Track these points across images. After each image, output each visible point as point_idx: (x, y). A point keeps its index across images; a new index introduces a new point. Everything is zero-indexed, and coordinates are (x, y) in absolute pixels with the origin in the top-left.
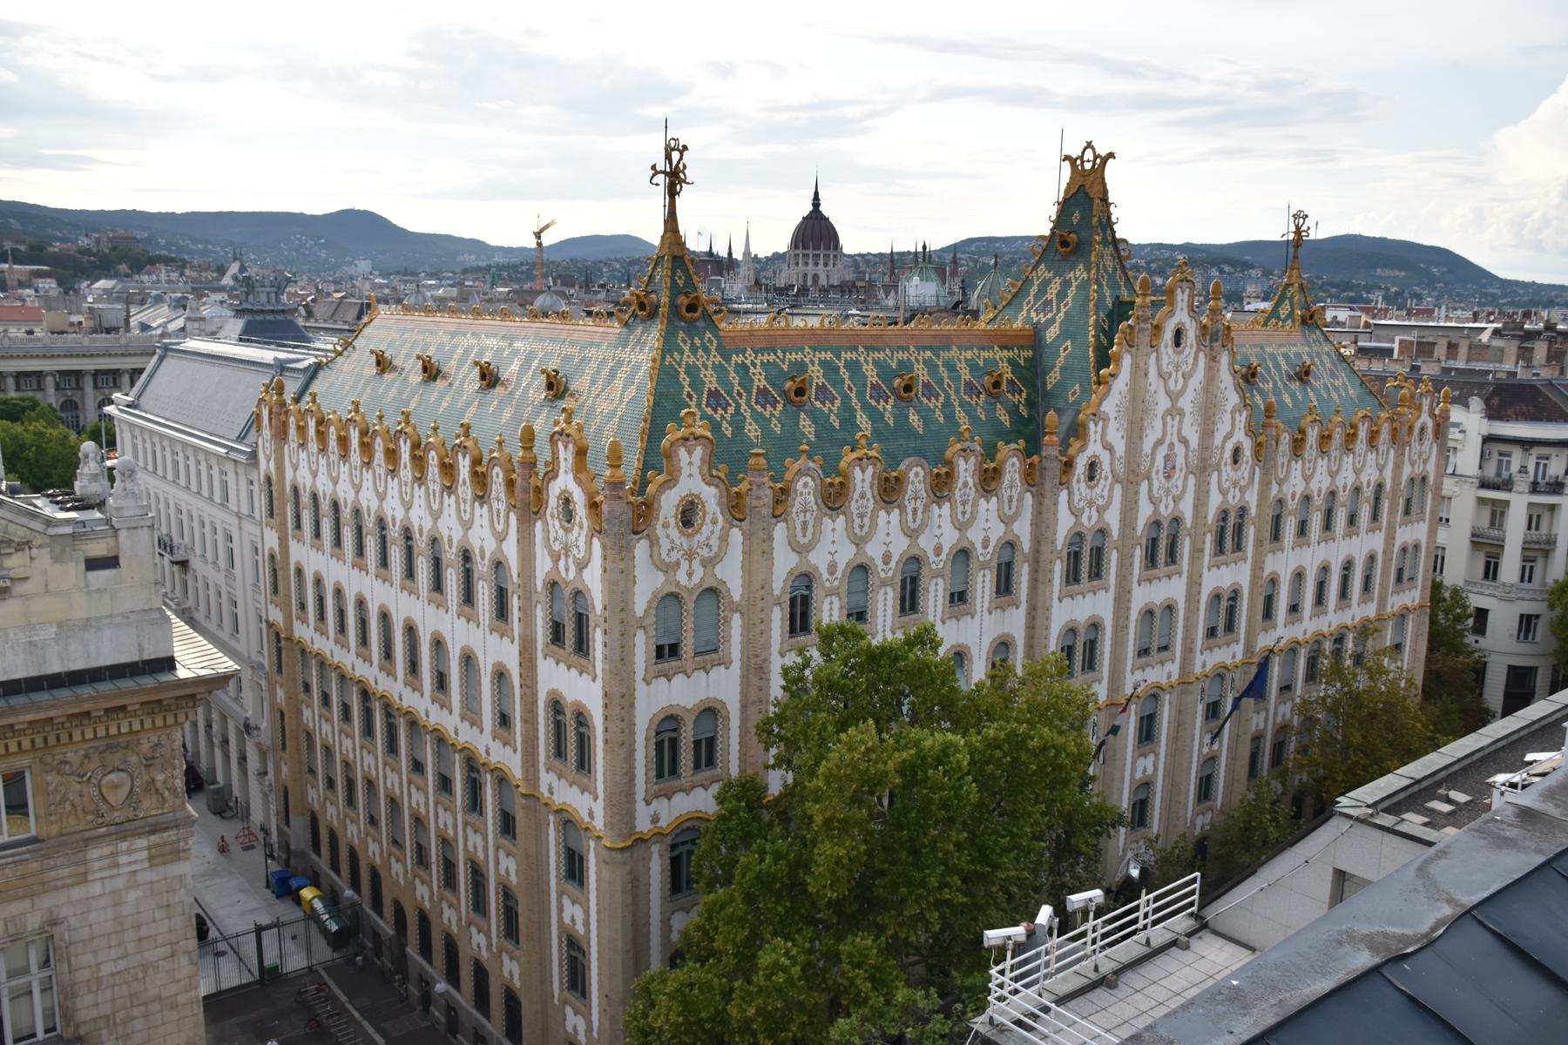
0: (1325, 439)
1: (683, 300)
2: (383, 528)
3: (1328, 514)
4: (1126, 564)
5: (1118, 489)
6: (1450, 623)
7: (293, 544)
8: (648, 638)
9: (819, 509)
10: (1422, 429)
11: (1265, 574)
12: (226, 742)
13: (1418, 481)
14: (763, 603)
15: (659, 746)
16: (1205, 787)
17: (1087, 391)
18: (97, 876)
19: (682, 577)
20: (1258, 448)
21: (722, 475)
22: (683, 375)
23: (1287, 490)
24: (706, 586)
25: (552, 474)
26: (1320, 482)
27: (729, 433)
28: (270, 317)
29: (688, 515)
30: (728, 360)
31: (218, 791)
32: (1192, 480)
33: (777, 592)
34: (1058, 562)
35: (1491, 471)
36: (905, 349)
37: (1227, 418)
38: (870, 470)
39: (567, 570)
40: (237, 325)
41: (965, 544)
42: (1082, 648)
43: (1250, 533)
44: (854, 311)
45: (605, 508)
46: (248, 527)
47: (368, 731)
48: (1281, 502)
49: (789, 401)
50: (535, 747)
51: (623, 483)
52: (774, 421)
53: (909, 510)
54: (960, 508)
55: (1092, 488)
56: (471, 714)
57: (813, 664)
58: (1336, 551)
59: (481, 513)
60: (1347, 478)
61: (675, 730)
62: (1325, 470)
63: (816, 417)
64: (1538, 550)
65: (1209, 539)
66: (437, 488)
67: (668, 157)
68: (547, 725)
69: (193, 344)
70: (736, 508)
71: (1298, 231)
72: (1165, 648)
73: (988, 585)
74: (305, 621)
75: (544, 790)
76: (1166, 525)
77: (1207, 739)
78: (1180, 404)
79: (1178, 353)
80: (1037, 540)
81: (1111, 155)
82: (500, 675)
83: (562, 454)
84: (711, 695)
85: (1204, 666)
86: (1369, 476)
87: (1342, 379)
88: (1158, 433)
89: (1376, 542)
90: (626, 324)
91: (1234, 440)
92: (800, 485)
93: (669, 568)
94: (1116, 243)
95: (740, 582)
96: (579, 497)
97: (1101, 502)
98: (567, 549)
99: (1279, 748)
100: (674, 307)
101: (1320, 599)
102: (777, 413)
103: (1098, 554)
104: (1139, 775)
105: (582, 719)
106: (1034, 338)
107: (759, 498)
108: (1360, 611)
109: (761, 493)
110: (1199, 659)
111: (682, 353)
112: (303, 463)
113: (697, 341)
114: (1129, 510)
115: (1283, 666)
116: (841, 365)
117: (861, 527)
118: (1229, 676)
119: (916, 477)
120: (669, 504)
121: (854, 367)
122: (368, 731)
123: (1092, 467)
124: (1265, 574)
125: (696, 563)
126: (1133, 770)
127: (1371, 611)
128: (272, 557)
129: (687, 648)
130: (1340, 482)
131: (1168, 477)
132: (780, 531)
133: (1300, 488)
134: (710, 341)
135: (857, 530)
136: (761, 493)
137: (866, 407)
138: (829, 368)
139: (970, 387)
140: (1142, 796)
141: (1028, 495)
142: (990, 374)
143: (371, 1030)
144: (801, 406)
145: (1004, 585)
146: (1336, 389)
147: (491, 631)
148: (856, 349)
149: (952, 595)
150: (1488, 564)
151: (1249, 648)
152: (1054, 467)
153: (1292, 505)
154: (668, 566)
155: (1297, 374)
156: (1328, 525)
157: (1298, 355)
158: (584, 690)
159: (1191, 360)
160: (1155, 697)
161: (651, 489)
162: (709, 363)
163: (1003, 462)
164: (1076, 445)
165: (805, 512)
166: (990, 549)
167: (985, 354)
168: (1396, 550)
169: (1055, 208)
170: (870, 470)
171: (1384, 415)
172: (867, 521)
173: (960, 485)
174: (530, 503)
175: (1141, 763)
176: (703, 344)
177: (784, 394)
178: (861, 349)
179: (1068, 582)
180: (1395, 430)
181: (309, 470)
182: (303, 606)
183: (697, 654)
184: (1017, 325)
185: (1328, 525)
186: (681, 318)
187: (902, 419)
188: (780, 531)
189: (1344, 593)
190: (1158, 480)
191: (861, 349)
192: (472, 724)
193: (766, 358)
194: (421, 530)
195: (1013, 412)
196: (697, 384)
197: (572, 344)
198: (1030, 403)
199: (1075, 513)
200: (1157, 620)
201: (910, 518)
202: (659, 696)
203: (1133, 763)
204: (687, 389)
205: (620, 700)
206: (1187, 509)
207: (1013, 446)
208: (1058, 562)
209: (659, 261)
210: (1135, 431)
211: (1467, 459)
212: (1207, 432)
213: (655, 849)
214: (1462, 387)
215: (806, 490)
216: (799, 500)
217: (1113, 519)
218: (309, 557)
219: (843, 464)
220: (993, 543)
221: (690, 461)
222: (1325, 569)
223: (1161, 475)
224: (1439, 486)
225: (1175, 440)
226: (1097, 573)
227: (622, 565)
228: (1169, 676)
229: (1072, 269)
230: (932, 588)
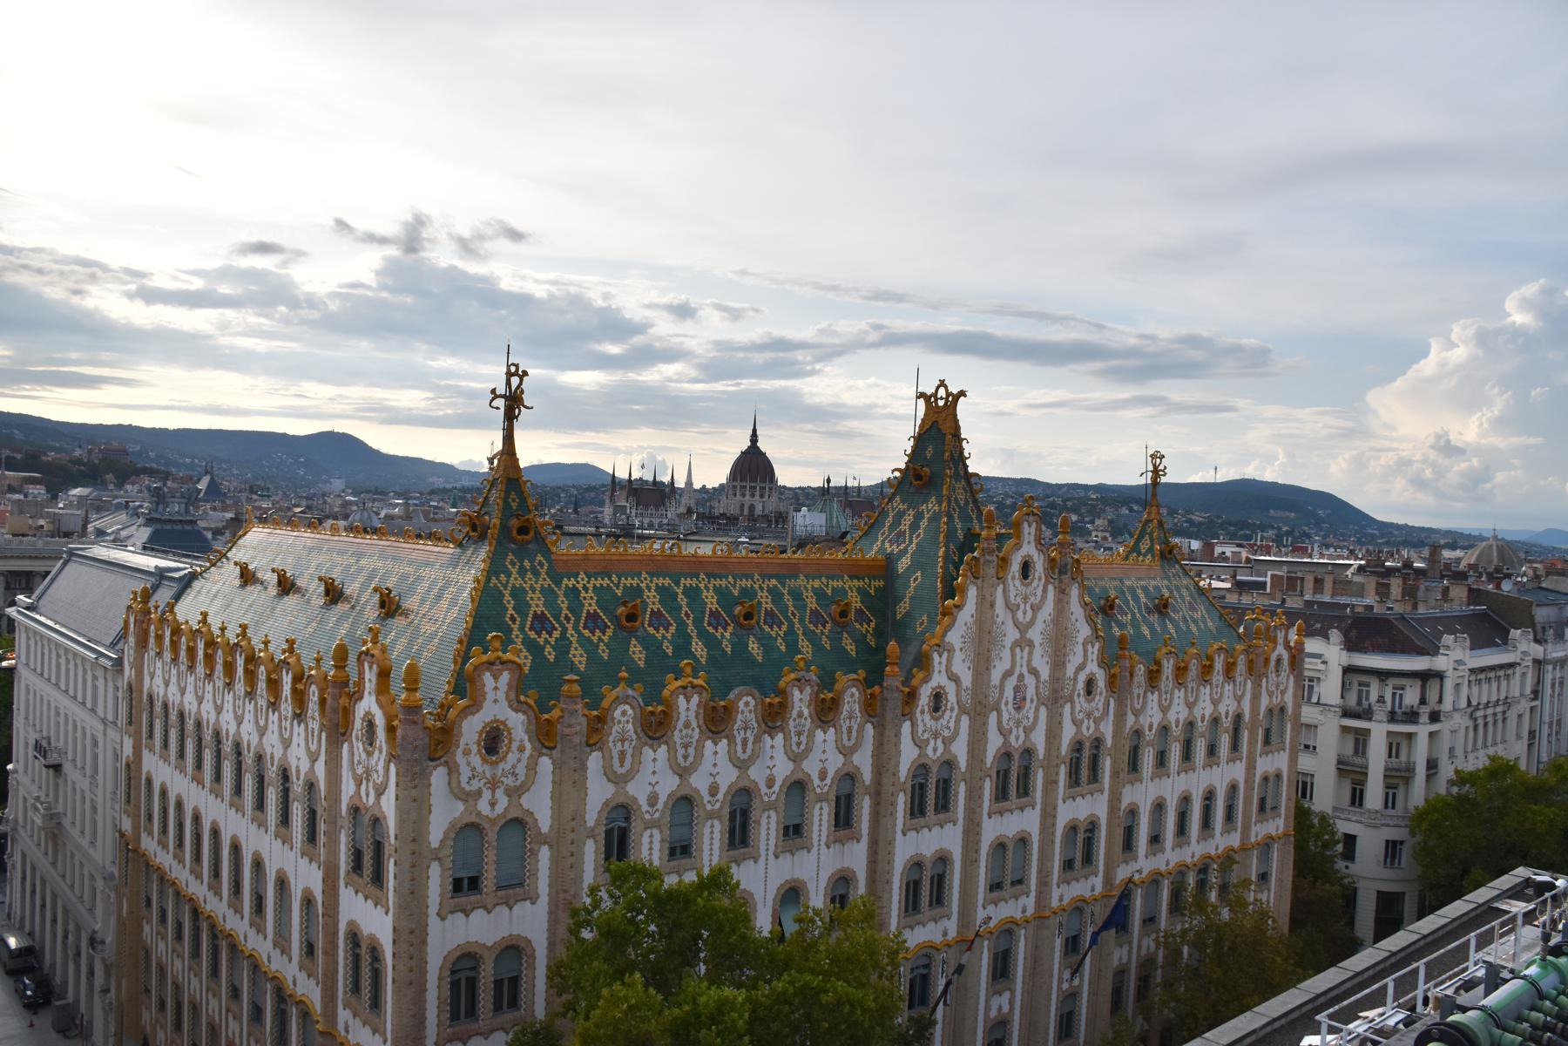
0: (1181, 671)
1: (514, 523)
2: (219, 742)
3: (1189, 744)
4: (974, 796)
6: (1315, 849)
7: (145, 752)
8: (443, 870)
9: (639, 738)
10: (1279, 661)
11: (1124, 805)
12: (78, 954)
13: (1276, 712)
14: (573, 836)
15: (455, 985)
16: (1067, 1024)
17: (933, 622)
19: (483, 806)
20: (1112, 681)
21: (531, 702)
22: (507, 597)
23: (1144, 721)
24: (511, 815)
25: (358, 696)
26: (1178, 713)
28: (179, 527)
29: (493, 741)
30: (558, 583)
31: (63, 1007)
32: (1043, 712)
33: (590, 824)
34: (901, 795)
35: (1352, 700)
36: (749, 576)
37: (1079, 649)
38: (695, 699)
40: (144, 533)
41: (800, 776)
42: (927, 887)
43: (1107, 765)
44: (743, 539)
45: (399, 732)
46: (112, 734)
47: (196, 953)
48: (1138, 733)
49: (620, 627)
50: (335, 981)
51: (420, 707)
53: (739, 741)
55: (937, 719)
56: (281, 942)
57: (603, 905)
58: (1197, 782)
60: (1205, 708)
61: (474, 969)
62: (1182, 701)
63: (649, 644)
64: (1398, 778)
65: (1063, 770)
67: (508, 383)
68: (346, 959)
69: (101, 552)
70: (545, 737)
71: (1156, 471)
72: (1020, 882)
73: (825, 818)
74: (150, 833)
75: (341, 1027)
76: (1017, 756)
77: (1067, 974)
78: (1030, 634)
80: (878, 771)
81: (962, 393)
82: (308, 901)
83: (367, 676)
84: (515, 932)
85: (1061, 899)
86: (1227, 706)
87: (1201, 612)
89: (1237, 771)
90: (460, 545)
91: (1087, 671)
92: (617, 713)
93: (470, 797)
94: (969, 477)
95: (549, 812)
96: (380, 720)
97: (946, 733)
98: (368, 772)
99: (1144, 982)
100: (504, 528)
101: (1182, 829)
102: (606, 638)
103: (945, 787)
104: (993, 1013)
105: (375, 952)
106: (886, 568)
107: (570, 726)
108: (1223, 841)
109: (573, 721)
110: (1055, 893)
111: (509, 575)
112: (159, 673)
113: (527, 564)
115: (1145, 898)
116: (680, 591)
117: (685, 757)
118: (1088, 910)
119: (746, 706)
120: (471, 729)
121: (693, 594)
122: (196, 953)
123: (938, 698)
124: (1124, 805)
125: (500, 793)
126: (988, 1009)
127: (1234, 840)
128: (128, 765)
130: (1197, 713)
131: (1018, 709)
132: (594, 761)
133: (1157, 719)
134: (541, 564)
135: (681, 760)
136: (573, 721)
137: (703, 634)
138: (666, 595)
139: (816, 617)
140: (999, 1036)
141: (869, 727)
142: (837, 603)
144: (632, 632)
145: (843, 819)
146: (1194, 621)
147: (303, 854)
149: (786, 829)
150: (1354, 790)
151: (1108, 881)
152: (895, 700)
153: (1149, 735)
154: (468, 794)
155: (1156, 607)
156: (1187, 755)
157: (1157, 588)
158: (375, 921)
159: (1039, 592)
160: (1010, 932)
161: (452, 713)
162: (538, 587)
163: (843, 691)
164: (920, 675)
165: (623, 741)
166: (828, 781)
167: (835, 583)
168: (1257, 779)
169: (912, 442)
170: (695, 699)
171: (1240, 647)
172: (691, 751)
173: (794, 714)
174: (338, 728)
176: (533, 567)
177: (615, 619)
178: (702, 576)
179: (912, 815)
181: (167, 682)
182: (150, 818)
183: (499, 888)
184: (870, 555)
185: (1187, 755)
186: (513, 540)
187: (740, 645)
188: (594, 761)
189: (1206, 823)
190: (1008, 711)
191: (702, 576)
192: (283, 953)
193: (600, 581)
195: (860, 641)
196: (522, 607)
197: (411, 563)
198: (880, 634)
199: (919, 744)
200: (1010, 853)
201: (739, 748)
202: (449, 934)
203: (987, 1001)
204: (511, 611)
205: (412, 935)
206: (1039, 739)
207: (854, 676)
208: (901, 795)
209: (493, 484)
210: (982, 664)
211: (1330, 689)
212: (1058, 663)
214: (1317, 621)
215: (624, 718)
216: (616, 728)
217: (960, 750)
218: (158, 768)
219: (666, 693)
220: (831, 774)
221: (496, 691)
222: (1186, 800)
223: (1010, 706)
224: (1297, 715)
226: (944, 805)
227: (414, 793)
228: (1024, 911)
229: (925, 501)
230: (764, 821)
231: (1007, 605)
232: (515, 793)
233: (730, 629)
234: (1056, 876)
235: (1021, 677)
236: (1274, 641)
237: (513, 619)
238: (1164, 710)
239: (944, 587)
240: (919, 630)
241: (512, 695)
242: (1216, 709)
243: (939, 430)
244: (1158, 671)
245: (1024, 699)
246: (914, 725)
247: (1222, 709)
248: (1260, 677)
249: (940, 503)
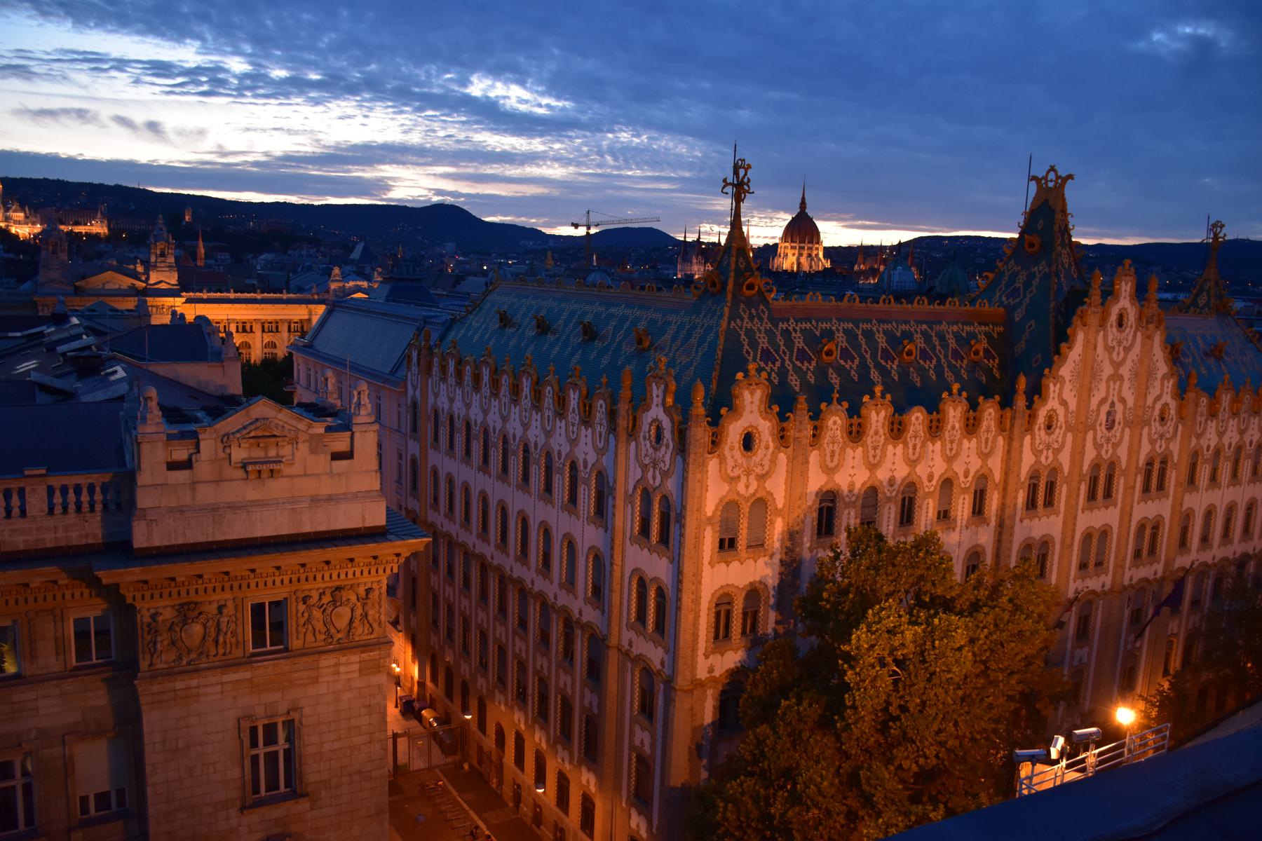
5: (1070, 436)
15: (718, 614)
18: (325, 679)
19: (741, 488)
22: (743, 337)
24: (758, 496)
27: (776, 381)
29: (748, 442)
30: (776, 326)
36: (907, 322)
37: (1157, 383)
38: (883, 413)
39: (654, 479)
43: (1172, 478)
48: (1196, 454)
52: (810, 374)
53: (910, 446)
54: (949, 446)
55: (1049, 435)
59: (585, 434)
61: (729, 603)
63: (840, 371)
66: (551, 414)
67: (736, 173)
70: (782, 437)
73: (966, 506)
77: (1132, 638)
80: (1006, 473)
81: (1070, 177)
85: (1131, 579)
88: (1102, 394)
91: (1162, 401)
96: (666, 423)
97: (1056, 446)
98: (655, 463)
103: (1051, 487)
111: (742, 320)
113: (753, 311)
114: (1078, 453)
116: (859, 333)
117: (874, 456)
121: (869, 335)
125: (752, 478)
129: (742, 543)
132: (814, 457)
137: (878, 366)
141: (1000, 440)
143: (476, 818)
148: (870, 321)
149: (939, 513)
151: (1167, 565)
154: (732, 478)
159: (1130, 338)
166: (970, 479)
167: (968, 328)
170: (883, 413)
172: (878, 452)
173: (949, 427)
175: (1078, 652)
179: (1028, 508)
183: (749, 547)
190: (1101, 430)
194: (536, 445)
196: (753, 344)
199: (1036, 453)
201: (911, 451)
210: (1085, 392)
213: (710, 692)
216: (829, 433)
217: (1065, 458)
220: (971, 474)
223: (1103, 428)
225: (1116, 400)
232: (762, 478)
234: (1128, 561)
235: (1113, 404)
237: (748, 352)
238: (1221, 434)
240: (1034, 365)
241: (763, 408)
246: (1033, 438)
249: (1050, 266)
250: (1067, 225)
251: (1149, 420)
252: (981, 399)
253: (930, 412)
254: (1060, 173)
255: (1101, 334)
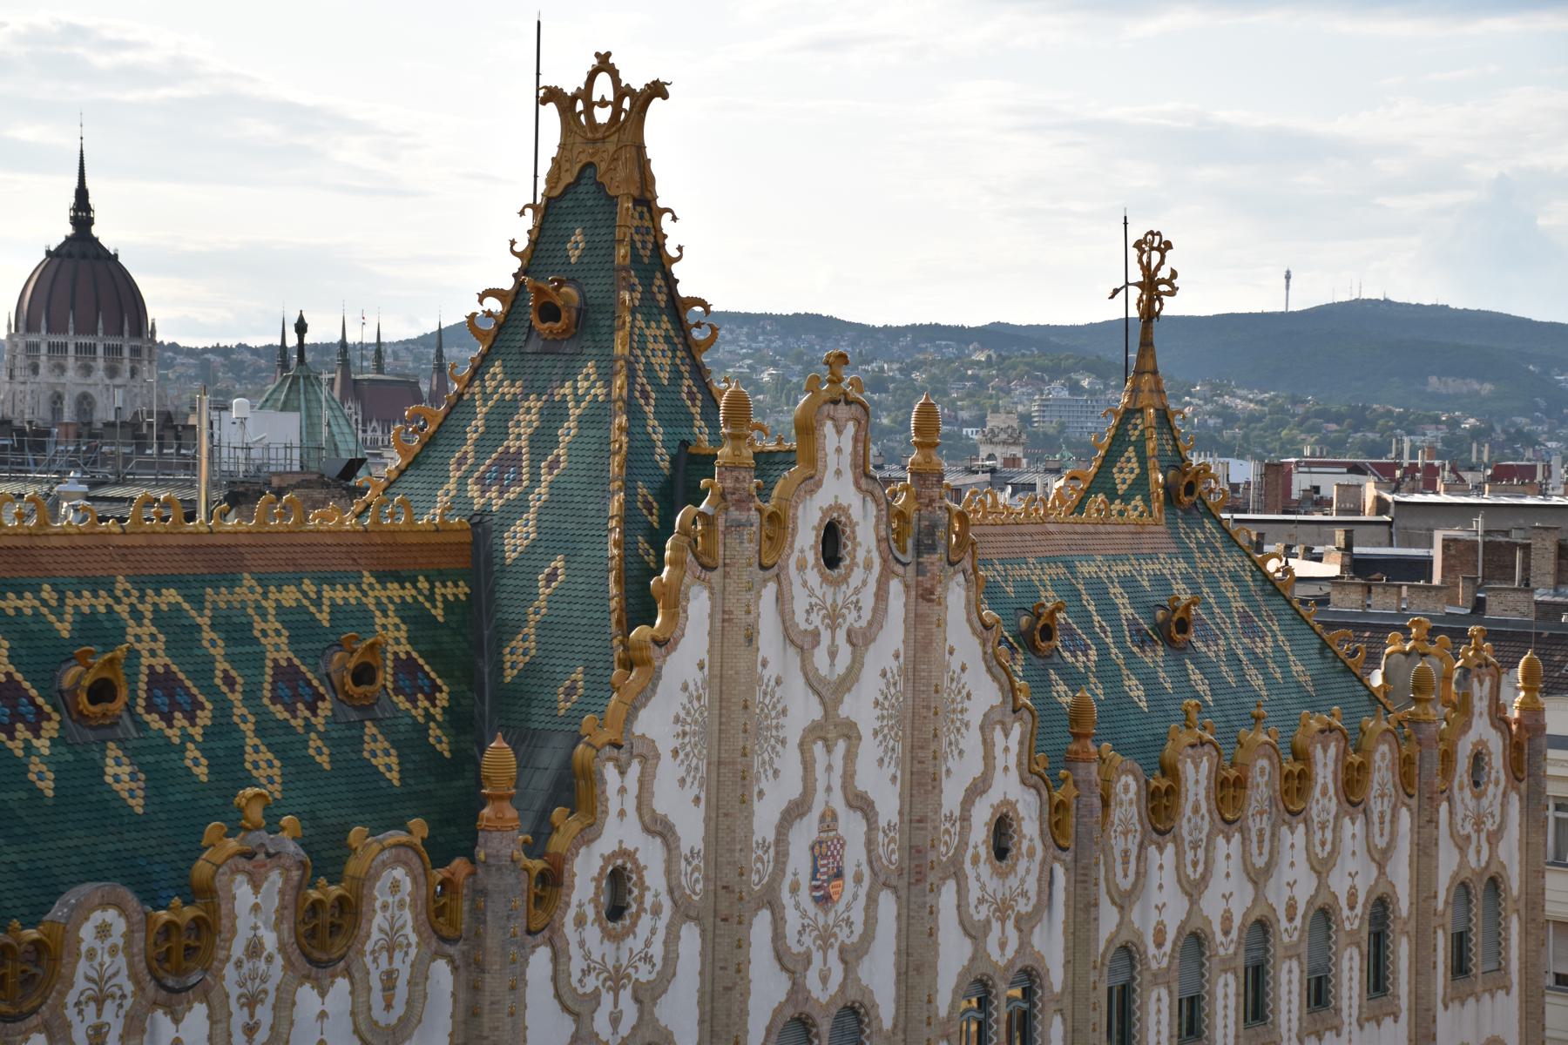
5: (690, 940)
10: (1478, 759)
13: (1478, 890)
17: (600, 685)
20: (1057, 820)
23: (1143, 920)
32: (888, 905)
37: (972, 740)
48: (1128, 953)
55: (617, 938)
60: (1294, 883)
62: (1235, 864)
71: (1152, 287)
76: (825, 1026)
78: (846, 709)
79: (835, 583)
81: (658, 89)
86: (1352, 878)
87: (1274, 637)
88: (794, 790)
91: (994, 796)
94: (677, 307)
97: (644, 974)
123: (619, 885)
130: (1277, 896)
131: (824, 901)
133: (1174, 913)
139: (289, 682)
141: (442, 975)
146: (1259, 662)
152: (509, 893)
153: (1158, 957)
157: (1160, 581)
159: (868, 600)
163: (371, 877)
167: (339, 594)
169: (528, 221)
173: (238, 949)
180: (1407, 762)
184: (431, 516)
187: (80, 773)
195: (410, 743)
198: (461, 721)
212: (921, 780)
223: (805, 895)
224: (1534, 898)
225: (838, 802)
229: (570, 374)
231: (789, 634)
233: (50, 728)
236: (1463, 707)
238: (1193, 890)
239: (626, 595)
240: (564, 706)
242: (1322, 884)
243: (599, 182)
244: (1173, 792)
245: (839, 875)
247: (1339, 884)
248: (1433, 803)
249: (607, 378)
250: (659, 239)
251: (772, 888)
252: (356, 834)
253: (151, 897)
254: (626, 79)
255: (770, 591)
